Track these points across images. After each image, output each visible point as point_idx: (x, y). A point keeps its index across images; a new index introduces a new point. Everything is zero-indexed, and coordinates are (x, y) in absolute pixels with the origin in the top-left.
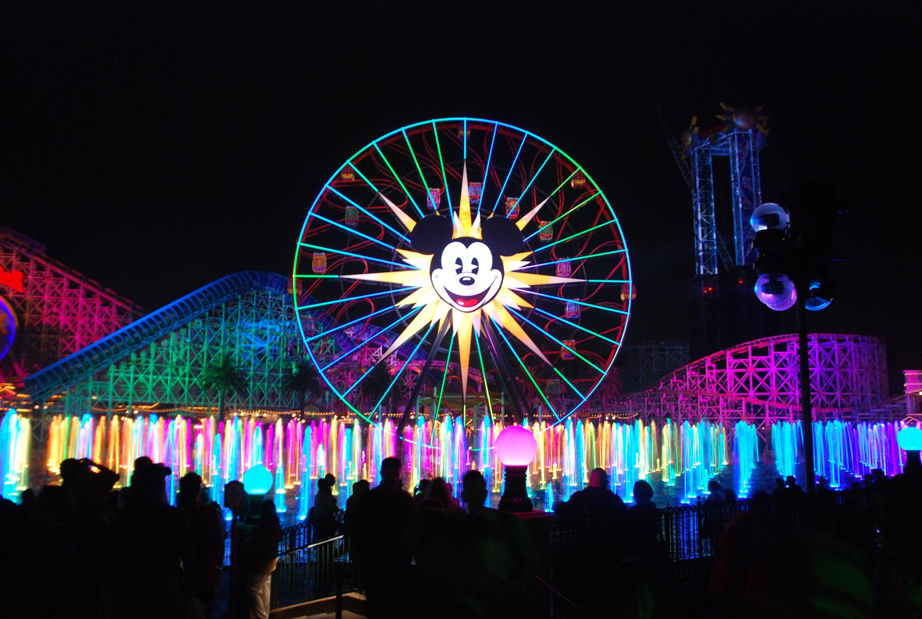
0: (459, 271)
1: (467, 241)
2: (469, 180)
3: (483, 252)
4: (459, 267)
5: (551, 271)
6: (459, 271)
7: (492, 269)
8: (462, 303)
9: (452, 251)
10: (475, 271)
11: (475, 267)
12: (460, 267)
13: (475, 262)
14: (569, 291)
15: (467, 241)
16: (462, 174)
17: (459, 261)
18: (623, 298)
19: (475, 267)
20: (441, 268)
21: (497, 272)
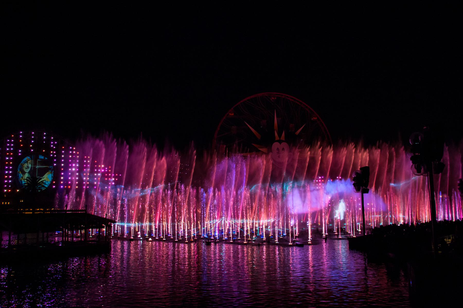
1: (280, 141)
2: (277, 117)
17: (278, 149)
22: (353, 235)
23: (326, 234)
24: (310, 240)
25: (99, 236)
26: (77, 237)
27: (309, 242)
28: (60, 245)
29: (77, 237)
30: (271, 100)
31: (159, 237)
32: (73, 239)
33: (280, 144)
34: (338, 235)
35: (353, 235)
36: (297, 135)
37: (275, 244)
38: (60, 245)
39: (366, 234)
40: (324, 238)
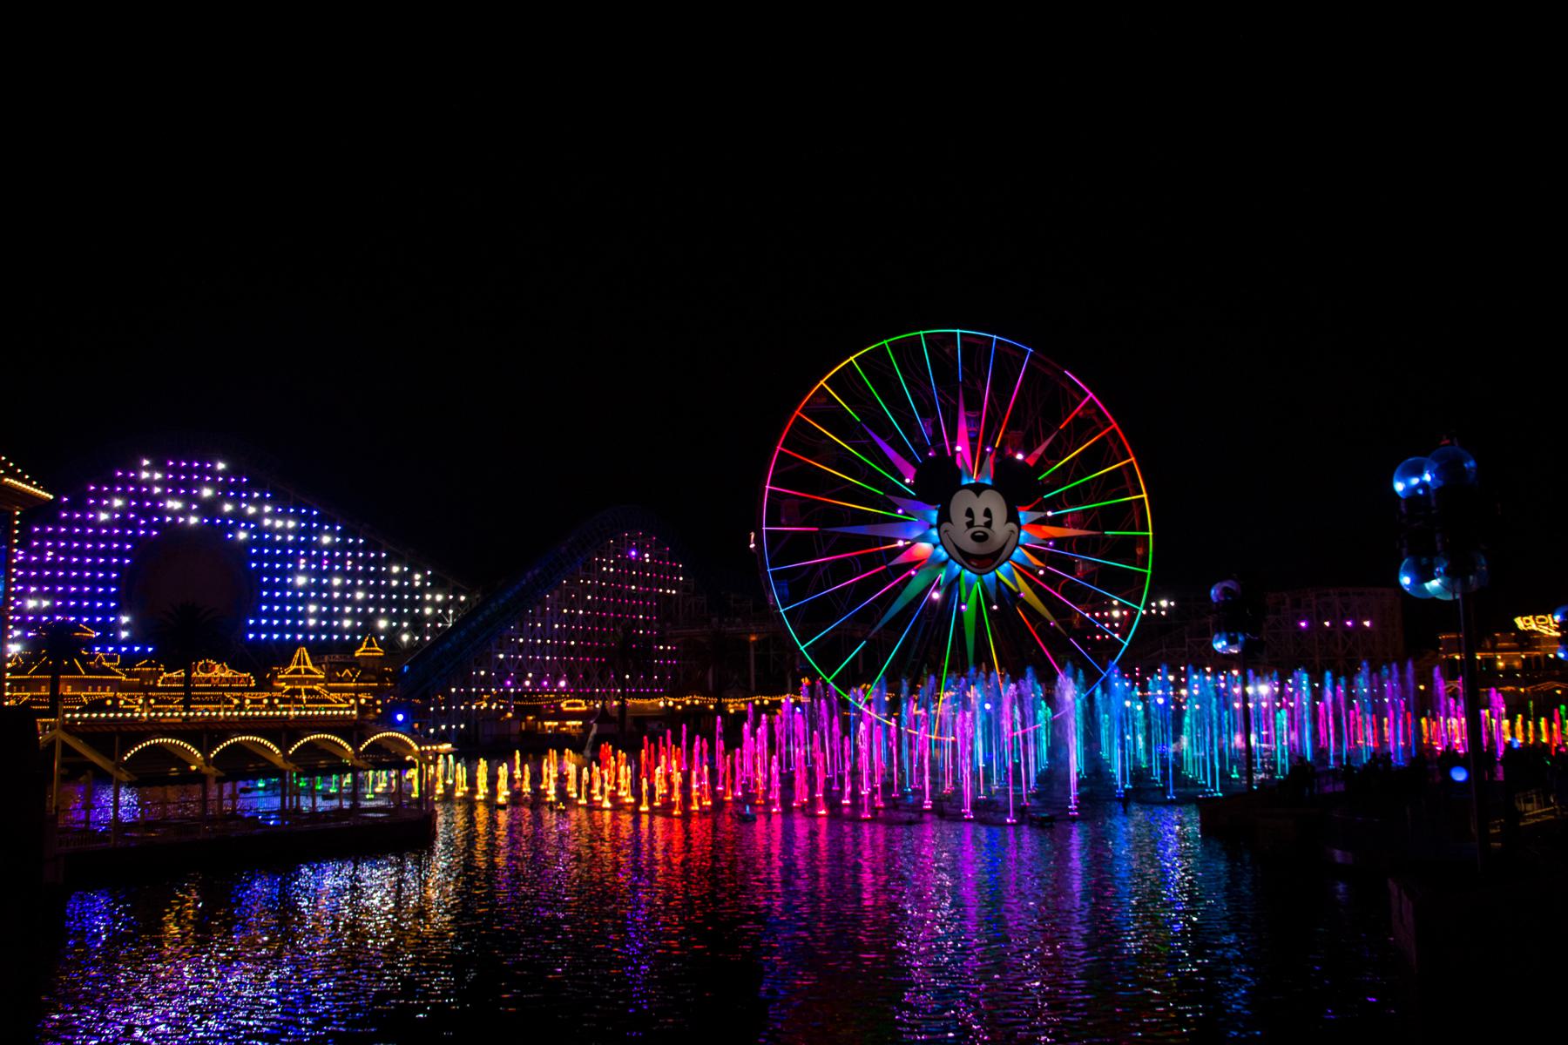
0: (970, 525)
1: (978, 489)
3: (994, 502)
4: (969, 519)
5: (1057, 521)
6: (970, 525)
7: (1008, 521)
8: (975, 564)
9: (962, 502)
10: (988, 525)
11: (987, 519)
12: (969, 519)
13: (987, 513)
14: (1081, 545)
15: (978, 489)
16: (957, 402)
18: (1139, 551)
19: (987, 519)
20: (950, 521)
21: (1012, 526)
22: (1216, 792)
23: (1126, 786)
24: (1076, 804)
25: (398, 793)
26: (328, 797)
27: (1071, 810)
28: (272, 823)
29: (328, 797)
30: (947, 351)
31: (590, 797)
32: (314, 803)
33: (978, 494)
34: (1164, 791)
35: (1216, 792)
36: (1031, 465)
37: (957, 818)
38: (272, 823)
39: (1255, 787)
40: (1119, 799)
